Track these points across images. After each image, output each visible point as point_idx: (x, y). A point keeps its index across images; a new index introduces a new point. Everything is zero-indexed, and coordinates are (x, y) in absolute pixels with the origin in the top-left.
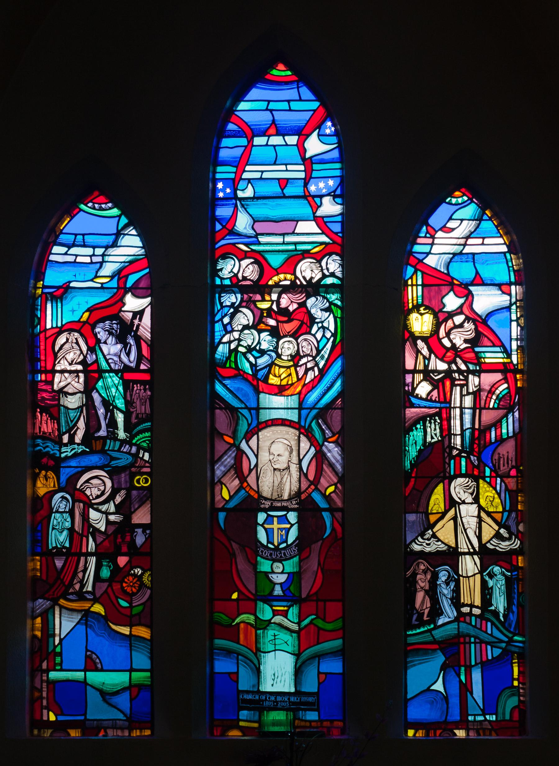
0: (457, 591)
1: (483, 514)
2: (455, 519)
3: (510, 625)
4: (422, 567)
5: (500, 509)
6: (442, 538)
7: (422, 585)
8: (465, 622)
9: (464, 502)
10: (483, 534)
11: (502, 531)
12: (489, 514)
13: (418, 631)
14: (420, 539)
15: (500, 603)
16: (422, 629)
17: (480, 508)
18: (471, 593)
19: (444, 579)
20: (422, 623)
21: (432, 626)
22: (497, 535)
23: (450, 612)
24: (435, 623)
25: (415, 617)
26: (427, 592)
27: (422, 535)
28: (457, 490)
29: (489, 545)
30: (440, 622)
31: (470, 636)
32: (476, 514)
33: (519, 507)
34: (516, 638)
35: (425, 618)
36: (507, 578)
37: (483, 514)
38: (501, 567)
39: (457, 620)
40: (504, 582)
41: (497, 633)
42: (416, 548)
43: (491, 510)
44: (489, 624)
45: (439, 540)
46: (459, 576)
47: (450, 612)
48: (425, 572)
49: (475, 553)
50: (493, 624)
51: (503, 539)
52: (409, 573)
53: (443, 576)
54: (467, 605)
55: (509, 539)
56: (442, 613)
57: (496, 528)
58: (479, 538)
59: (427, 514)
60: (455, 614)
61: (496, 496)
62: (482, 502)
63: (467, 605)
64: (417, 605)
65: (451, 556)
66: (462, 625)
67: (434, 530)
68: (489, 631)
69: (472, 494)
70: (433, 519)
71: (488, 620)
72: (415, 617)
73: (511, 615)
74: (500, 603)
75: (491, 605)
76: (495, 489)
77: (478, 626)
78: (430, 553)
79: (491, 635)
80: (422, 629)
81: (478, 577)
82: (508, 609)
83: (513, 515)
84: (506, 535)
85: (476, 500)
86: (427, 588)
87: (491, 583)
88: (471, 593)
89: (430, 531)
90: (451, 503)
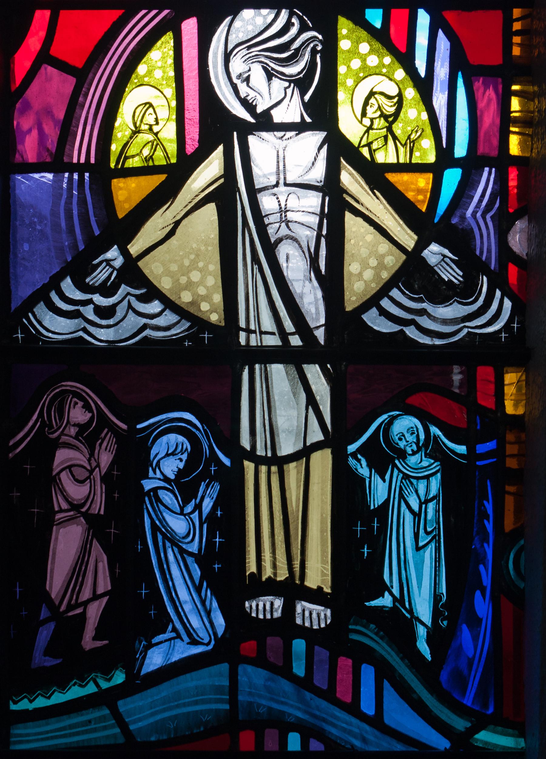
0: (227, 523)
1: (349, 178)
2: (223, 196)
3: (461, 680)
4: (79, 415)
5: (426, 151)
6: (165, 285)
7: (77, 492)
8: (260, 661)
9: (265, 122)
10: (352, 267)
11: (434, 252)
12: (376, 176)
13: (58, 698)
14: (67, 286)
15: (417, 579)
16: (75, 692)
17: (339, 149)
18: (295, 533)
19: (171, 467)
20: (74, 664)
21: (119, 678)
22: (413, 274)
23: (195, 613)
24: (131, 662)
25: (44, 634)
26: (96, 526)
27: (79, 268)
28: (237, 65)
29: (373, 320)
30: (155, 659)
31: (285, 727)
32: (318, 174)
33: (515, 146)
34: (485, 737)
35: (88, 641)
36: (453, 473)
37: (349, 178)
38: (425, 418)
39: (225, 650)
40: (435, 484)
41: (400, 716)
42: (56, 327)
43: (386, 155)
44: (368, 673)
45: (152, 293)
46: (240, 455)
47: (195, 613)
48: (89, 436)
49: (310, 352)
50: (384, 672)
51: (439, 292)
52: (22, 438)
53: (168, 456)
54: (272, 587)
55: (464, 291)
56: (162, 622)
57: (408, 239)
58: (332, 281)
59: (103, 172)
60: (220, 621)
61: (410, 93)
62: (350, 127)
63: (272, 587)
64: (56, 581)
65: (205, 364)
66: (252, 676)
67: (135, 248)
68: (368, 706)
69: (301, 83)
70: (127, 193)
71: (363, 655)
72: (44, 634)
73: (465, 633)
74: (417, 579)
75: (382, 588)
76: (406, 59)
77: (320, 680)
78: (112, 350)
79: (377, 721)
80: (75, 692)
81: (322, 463)
82: (452, 607)
83: (487, 179)
84: (451, 274)
85: (321, 112)
86: (98, 506)
87: (379, 491)
88: (295, 533)
89: (113, 253)
90: (218, 126)
